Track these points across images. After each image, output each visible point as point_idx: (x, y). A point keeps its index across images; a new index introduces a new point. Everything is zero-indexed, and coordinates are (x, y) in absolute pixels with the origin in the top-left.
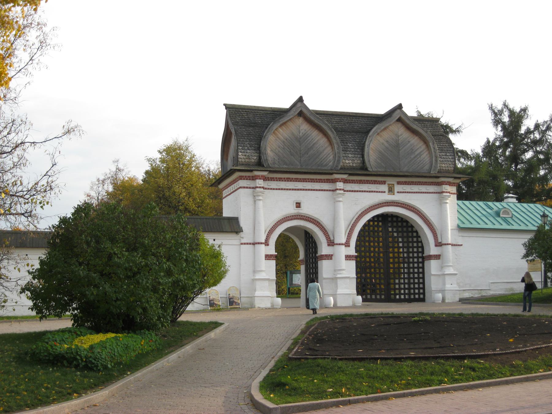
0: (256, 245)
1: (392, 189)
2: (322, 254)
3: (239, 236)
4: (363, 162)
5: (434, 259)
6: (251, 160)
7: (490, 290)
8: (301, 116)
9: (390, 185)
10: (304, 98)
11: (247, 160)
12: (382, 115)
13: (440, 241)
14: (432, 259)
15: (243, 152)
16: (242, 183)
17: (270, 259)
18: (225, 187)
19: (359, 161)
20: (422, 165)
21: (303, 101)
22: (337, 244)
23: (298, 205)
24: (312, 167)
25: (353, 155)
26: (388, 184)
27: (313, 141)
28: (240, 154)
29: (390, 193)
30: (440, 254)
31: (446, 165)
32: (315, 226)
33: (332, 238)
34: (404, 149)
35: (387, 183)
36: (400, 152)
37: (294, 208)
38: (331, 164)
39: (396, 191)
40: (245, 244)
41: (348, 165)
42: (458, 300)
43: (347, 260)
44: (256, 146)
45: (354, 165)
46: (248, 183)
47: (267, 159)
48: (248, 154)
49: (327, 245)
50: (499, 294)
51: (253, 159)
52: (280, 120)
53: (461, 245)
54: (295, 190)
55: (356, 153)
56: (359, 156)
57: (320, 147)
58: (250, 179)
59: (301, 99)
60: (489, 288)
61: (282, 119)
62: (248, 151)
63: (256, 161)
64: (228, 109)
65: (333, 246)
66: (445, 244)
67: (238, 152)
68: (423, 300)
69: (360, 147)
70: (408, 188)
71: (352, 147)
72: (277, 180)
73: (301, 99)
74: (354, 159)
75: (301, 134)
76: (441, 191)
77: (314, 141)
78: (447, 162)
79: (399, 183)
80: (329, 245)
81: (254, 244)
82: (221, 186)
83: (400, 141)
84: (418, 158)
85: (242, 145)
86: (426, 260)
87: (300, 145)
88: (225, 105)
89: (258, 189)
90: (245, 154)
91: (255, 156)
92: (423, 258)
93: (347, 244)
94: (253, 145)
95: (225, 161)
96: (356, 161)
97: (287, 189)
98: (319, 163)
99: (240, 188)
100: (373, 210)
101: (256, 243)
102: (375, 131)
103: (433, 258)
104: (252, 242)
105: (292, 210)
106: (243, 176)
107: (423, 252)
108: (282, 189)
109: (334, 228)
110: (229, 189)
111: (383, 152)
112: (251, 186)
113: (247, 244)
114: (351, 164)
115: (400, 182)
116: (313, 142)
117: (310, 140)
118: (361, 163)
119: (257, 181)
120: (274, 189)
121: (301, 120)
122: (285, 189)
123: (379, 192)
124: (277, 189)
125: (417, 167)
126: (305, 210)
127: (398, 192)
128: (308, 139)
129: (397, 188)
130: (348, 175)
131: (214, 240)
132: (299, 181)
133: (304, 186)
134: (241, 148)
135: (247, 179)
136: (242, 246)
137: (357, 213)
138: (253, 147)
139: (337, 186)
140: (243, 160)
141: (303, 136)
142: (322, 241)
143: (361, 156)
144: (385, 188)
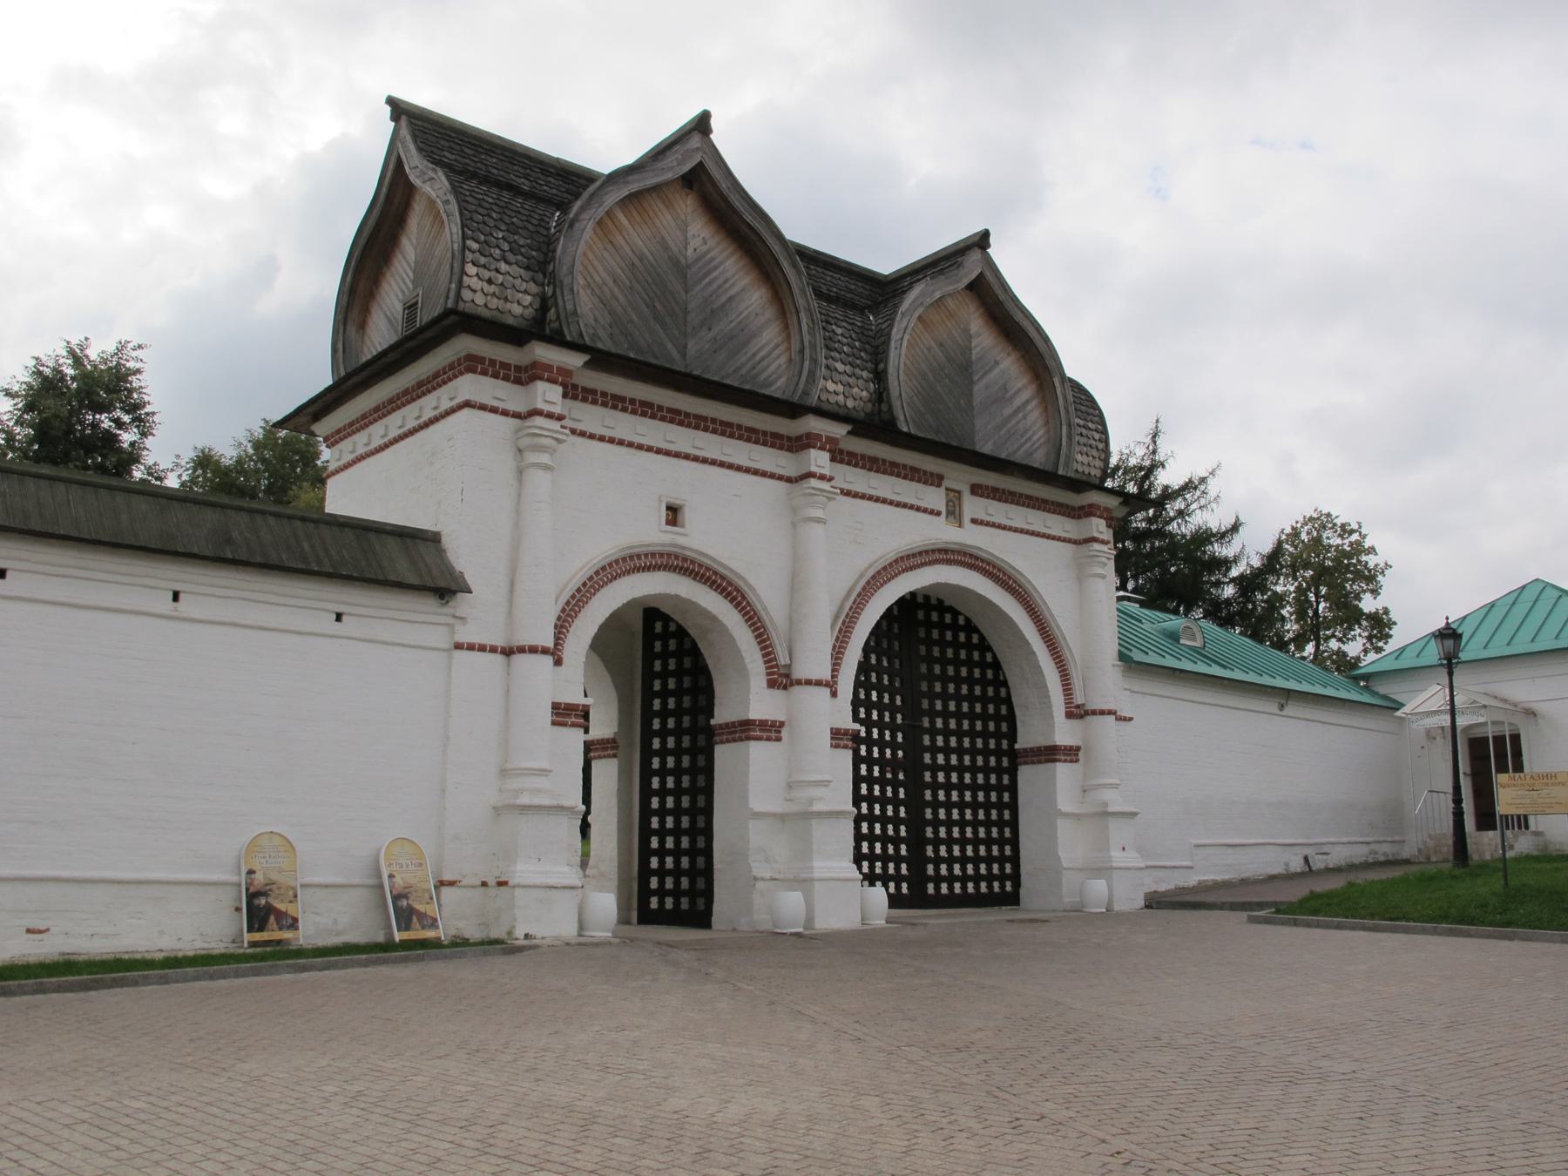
0: (519, 659)
1: (954, 506)
2: (752, 716)
3: (451, 611)
4: (881, 395)
5: (1065, 761)
6: (509, 306)
7: (1191, 868)
8: (691, 188)
9: (952, 494)
10: (714, 123)
11: (494, 303)
12: (886, 276)
13: (1079, 700)
14: (1060, 761)
15: (484, 266)
16: (469, 386)
17: (564, 724)
18: (351, 424)
19: (864, 394)
20: (1029, 444)
21: (711, 131)
22: (799, 682)
23: (674, 514)
24: (723, 378)
25: (848, 369)
26: (947, 489)
27: (727, 285)
28: (471, 269)
29: (951, 518)
31: (1085, 456)
32: (730, 606)
33: (783, 659)
34: (984, 381)
35: (946, 483)
36: (976, 388)
37: (660, 524)
38: (781, 382)
39: (967, 515)
40: (471, 647)
41: (833, 399)
42: (1142, 903)
43: (837, 746)
44: (534, 253)
45: (850, 403)
46: (500, 394)
47: (575, 313)
48: (501, 277)
49: (765, 684)
50: (1213, 880)
51: (519, 303)
52: (630, 178)
54: (668, 453)
55: (858, 362)
56: (865, 374)
57: (747, 317)
58: (506, 378)
59: (702, 124)
60: (1188, 863)
61: (636, 177)
62: (503, 267)
63: (529, 312)
64: (404, 119)
65: (785, 688)
66: (1094, 713)
67: (463, 262)
68: (1012, 899)
69: (867, 346)
71: (845, 340)
72: (605, 405)
73: (702, 124)
74: (851, 380)
75: (690, 251)
76: (1088, 535)
77: (733, 285)
79: (976, 490)
80: (772, 684)
81: (508, 652)
82: (323, 428)
83: (974, 352)
85: (482, 238)
86: (1021, 764)
87: (687, 293)
88: (391, 101)
89: (539, 421)
90: (493, 274)
91: (526, 292)
93: (831, 686)
94: (523, 250)
95: (352, 330)
96: (855, 390)
97: (640, 447)
98: (744, 371)
99: (467, 404)
100: (911, 568)
101: (521, 650)
102: (915, 300)
103: (1029, 759)
104: (500, 642)
105: (652, 533)
106: (480, 360)
107: (1012, 735)
108: (621, 443)
109: (792, 622)
112: (512, 407)
113: (482, 648)
114: (841, 398)
116: (727, 290)
117: (720, 281)
118: (870, 401)
119: (541, 386)
120: (592, 436)
121: (687, 205)
122: (630, 445)
123: (925, 511)
124: (602, 439)
125: (1018, 449)
126: (697, 538)
127: (974, 521)
129: (973, 506)
130: (849, 428)
131: (339, 617)
132: (681, 424)
133: (698, 444)
134: (475, 246)
135: (495, 376)
136: (459, 654)
137: (861, 576)
138: (522, 254)
139: (813, 462)
140: (480, 300)
141: (698, 259)
143: (871, 376)
144: (934, 497)
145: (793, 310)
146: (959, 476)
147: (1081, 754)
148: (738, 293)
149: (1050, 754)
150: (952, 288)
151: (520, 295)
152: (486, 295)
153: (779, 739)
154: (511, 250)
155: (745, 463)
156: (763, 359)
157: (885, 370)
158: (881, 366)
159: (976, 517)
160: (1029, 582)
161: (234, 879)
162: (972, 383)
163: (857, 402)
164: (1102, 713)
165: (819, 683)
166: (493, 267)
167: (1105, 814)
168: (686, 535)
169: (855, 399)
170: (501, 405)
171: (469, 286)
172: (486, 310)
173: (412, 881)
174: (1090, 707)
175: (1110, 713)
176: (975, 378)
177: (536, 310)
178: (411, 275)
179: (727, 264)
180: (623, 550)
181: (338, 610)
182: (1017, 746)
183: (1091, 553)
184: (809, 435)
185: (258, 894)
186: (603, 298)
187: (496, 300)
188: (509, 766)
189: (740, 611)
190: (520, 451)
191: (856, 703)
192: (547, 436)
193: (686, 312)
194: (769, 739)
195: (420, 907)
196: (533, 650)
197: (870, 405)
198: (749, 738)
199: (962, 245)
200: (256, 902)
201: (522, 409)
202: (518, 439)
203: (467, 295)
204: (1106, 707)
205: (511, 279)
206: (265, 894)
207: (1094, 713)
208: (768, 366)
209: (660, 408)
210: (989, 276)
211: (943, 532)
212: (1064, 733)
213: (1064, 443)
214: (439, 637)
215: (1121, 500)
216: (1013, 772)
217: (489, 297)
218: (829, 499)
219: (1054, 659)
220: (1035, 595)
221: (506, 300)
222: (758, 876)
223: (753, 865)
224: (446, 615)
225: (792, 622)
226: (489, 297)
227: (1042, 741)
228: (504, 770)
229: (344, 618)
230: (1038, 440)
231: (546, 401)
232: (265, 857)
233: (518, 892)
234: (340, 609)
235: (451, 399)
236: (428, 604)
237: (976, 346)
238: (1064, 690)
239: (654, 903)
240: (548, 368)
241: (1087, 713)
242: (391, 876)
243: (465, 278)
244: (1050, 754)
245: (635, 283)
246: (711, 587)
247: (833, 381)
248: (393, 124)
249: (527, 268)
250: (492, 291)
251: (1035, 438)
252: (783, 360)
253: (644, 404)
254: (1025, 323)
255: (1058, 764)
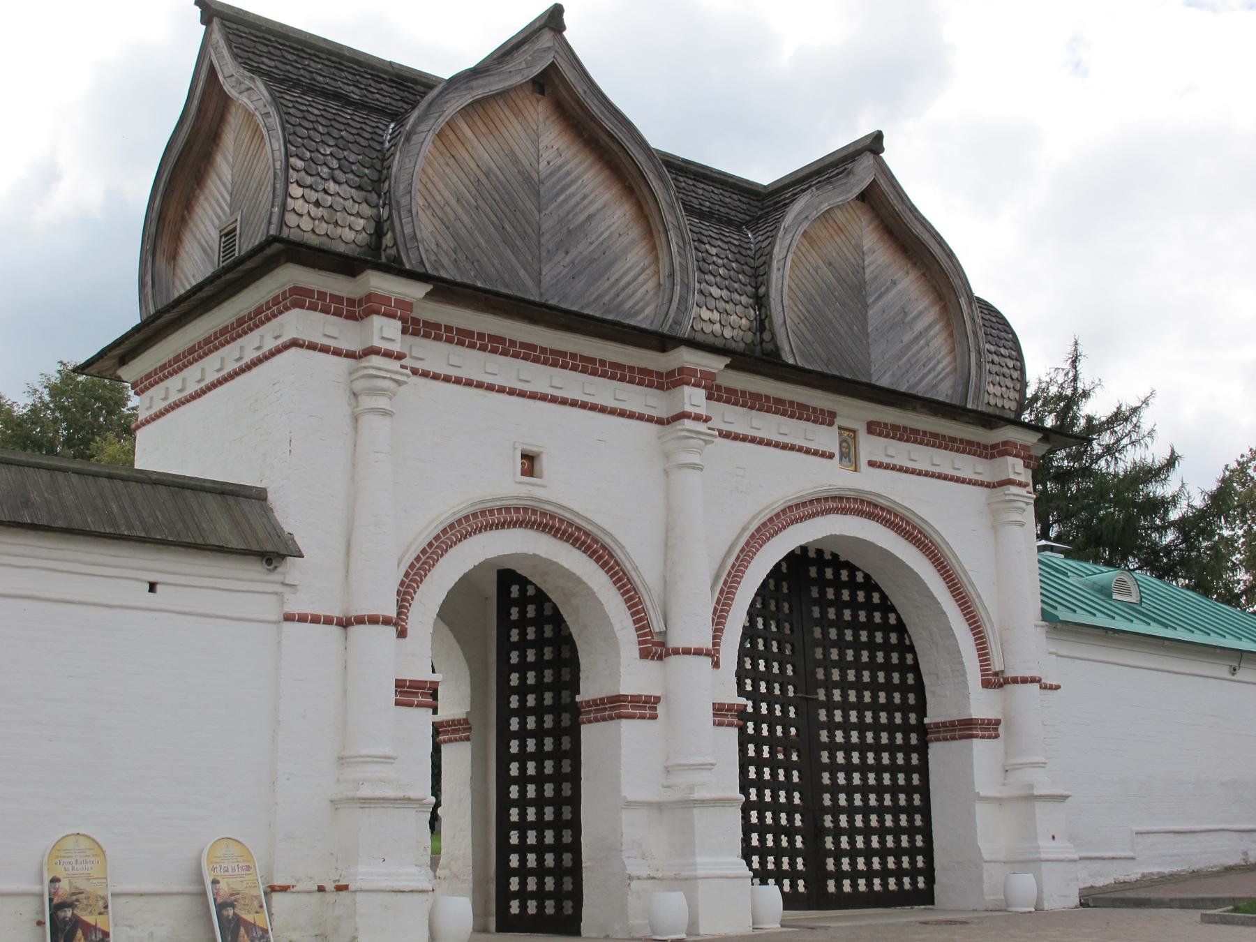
0: (356, 630)
1: (848, 447)
2: (623, 691)
4: (762, 324)
5: (983, 737)
6: (339, 230)
7: (1133, 859)
8: (542, 93)
9: (846, 434)
10: (567, 18)
11: (323, 228)
12: (765, 187)
13: (997, 666)
14: (976, 736)
15: (311, 187)
16: (295, 323)
17: (410, 705)
18: (163, 367)
19: (744, 321)
21: (564, 28)
22: (676, 652)
23: (530, 462)
24: (582, 307)
25: (725, 293)
26: (840, 428)
27: (586, 202)
28: (296, 191)
29: (845, 461)
30: (999, 717)
31: (997, 387)
33: (657, 626)
34: (880, 303)
35: (839, 421)
36: (870, 312)
37: (514, 475)
38: (649, 310)
40: (303, 619)
41: (708, 328)
42: (1077, 901)
43: (720, 724)
44: (367, 171)
45: (728, 333)
47: (414, 237)
48: (330, 198)
50: (1159, 873)
51: (351, 228)
52: (474, 83)
53: (1058, 687)
54: (522, 394)
55: (736, 285)
56: (744, 299)
57: (610, 237)
58: (338, 313)
59: (553, 20)
60: (1131, 854)
61: (480, 82)
62: (332, 187)
63: (363, 238)
64: (216, 21)
65: (660, 658)
66: (1015, 681)
67: (287, 183)
68: (926, 898)
69: (745, 268)
70: (900, 452)
71: (720, 262)
72: (450, 340)
73: (553, 20)
74: (729, 307)
75: (543, 164)
76: (1004, 478)
77: (592, 202)
78: (1002, 378)
79: (873, 428)
80: (645, 654)
81: (345, 623)
82: (131, 372)
83: (868, 271)
84: (922, 348)
85: (308, 155)
86: (932, 741)
87: (540, 212)
89: (375, 360)
90: (321, 195)
91: (358, 215)
92: (923, 730)
93: (713, 655)
94: (354, 168)
95: (161, 263)
96: (734, 317)
97: (490, 388)
98: (606, 299)
99: (294, 343)
100: (801, 519)
101: (360, 621)
103: (941, 735)
104: (336, 613)
107: (921, 708)
108: (469, 383)
110: (195, 369)
111: (820, 302)
112: (344, 345)
113: (315, 620)
114: (717, 327)
115: (878, 424)
117: (577, 198)
119: (377, 321)
120: (436, 377)
121: (538, 112)
122: (480, 385)
123: (816, 453)
124: (447, 379)
127: (872, 464)
128: (568, 192)
129: (870, 447)
130: (728, 361)
131: (152, 587)
132: (536, 360)
134: (300, 164)
135: (325, 311)
137: (744, 529)
138: (352, 172)
139: (686, 401)
140: (306, 224)
141: (551, 175)
142: (619, 634)
143: (751, 301)
144: (826, 438)
145: (661, 229)
146: (854, 412)
147: (1001, 729)
148: (599, 211)
149: (965, 729)
150: (840, 199)
151: (352, 218)
152: (314, 219)
153: (654, 717)
154: (340, 168)
155: (611, 403)
156: (629, 284)
157: (767, 295)
158: (762, 290)
159: (874, 459)
160: (936, 532)
161: (36, 888)
162: (866, 306)
163: (736, 332)
164: (1024, 680)
165: (698, 652)
166: (321, 187)
167: (1030, 798)
168: (544, 486)
169: (733, 328)
170: (332, 344)
171: (294, 209)
172: (314, 237)
173: (239, 887)
174: (1010, 674)
175: (1034, 680)
176: (870, 301)
177: (370, 235)
178: (228, 198)
179: (585, 178)
180: (472, 505)
181: (152, 579)
182: (926, 721)
183: (1008, 498)
184: (681, 370)
185: (63, 905)
186: (445, 219)
187: (324, 225)
188: (347, 753)
189: (607, 572)
190: (355, 395)
191: (741, 675)
192: (384, 378)
193: (540, 235)
194: (642, 717)
195: (249, 917)
196: (374, 620)
197: (750, 334)
198: (620, 717)
199: (851, 150)
200: (61, 914)
201: (356, 347)
202: (351, 381)
203: (291, 219)
204: (1028, 674)
205: (341, 200)
206: (71, 905)
207: (1015, 681)
208: (633, 294)
209: (513, 343)
210: (882, 182)
211: (834, 477)
212: (981, 705)
213: (973, 372)
214: (268, 608)
215: (1040, 435)
216: (923, 750)
217: (317, 222)
218: (706, 442)
219: (967, 620)
220: (944, 547)
221: (336, 224)
222: (634, 873)
223: (627, 862)
224: (276, 582)
225: (666, 584)
226: (317, 222)
227: (956, 715)
228: (342, 758)
229: (159, 588)
230: (943, 370)
231: (383, 338)
232: (71, 863)
233: (359, 896)
234: (153, 579)
235: (276, 338)
236: (253, 571)
237: (869, 265)
238: (980, 656)
239: (515, 907)
240: (386, 300)
241: (1006, 681)
242: (215, 882)
243: (289, 200)
244: (965, 729)
245: (481, 203)
246: (573, 544)
247: (708, 309)
248: (204, 27)
249: (359, 188)
250: (320, 215)
251: (940, 367)
252: (650, 285)
253: (493, 338)
254: (926, 237)
255: (975, 740)
